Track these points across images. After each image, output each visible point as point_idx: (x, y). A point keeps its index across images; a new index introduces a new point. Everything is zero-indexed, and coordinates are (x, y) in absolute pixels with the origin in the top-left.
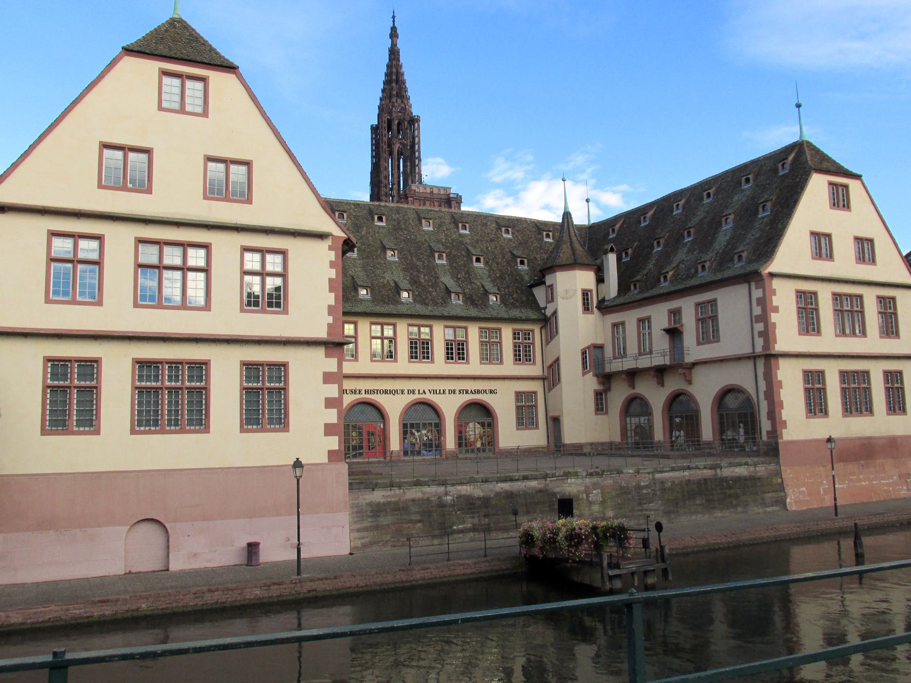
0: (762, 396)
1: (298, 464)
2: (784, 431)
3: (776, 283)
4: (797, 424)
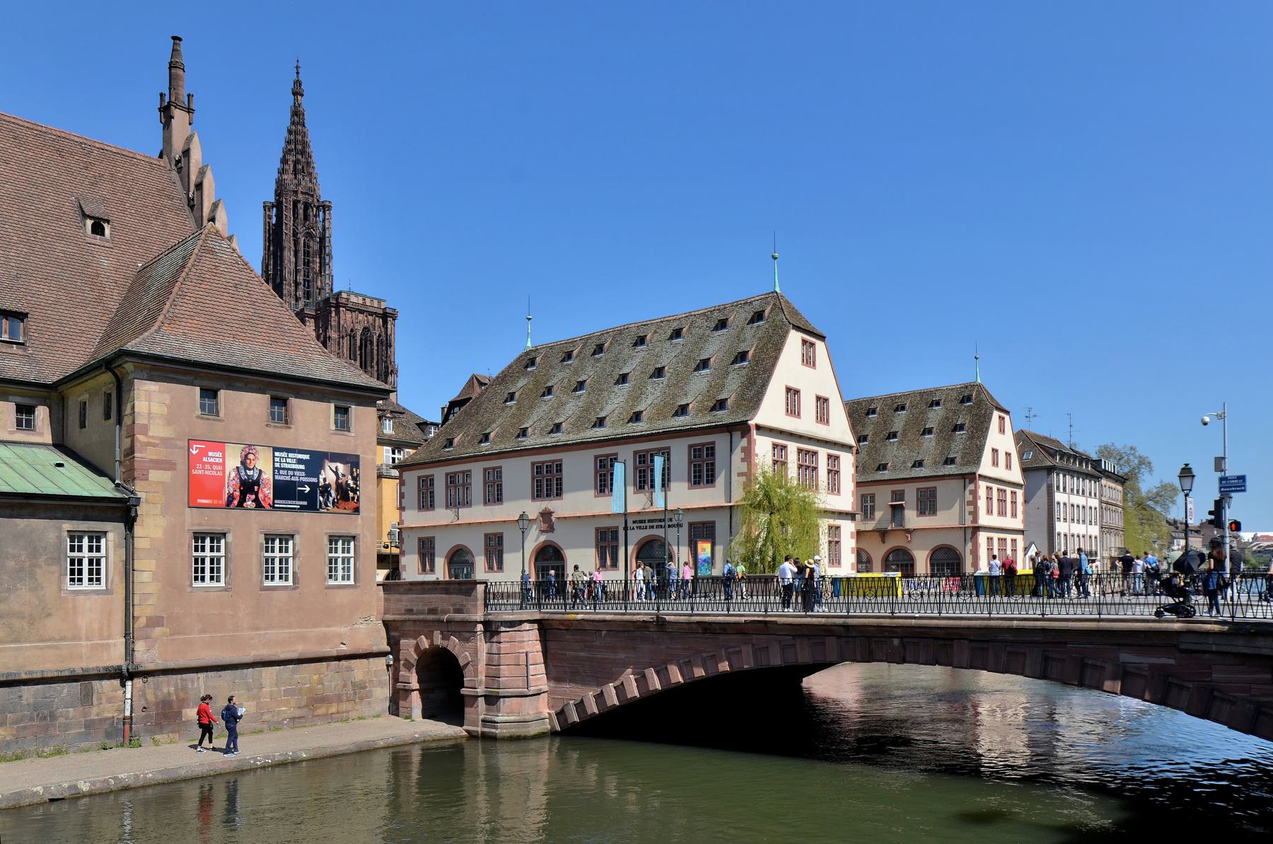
0: (968, 552)
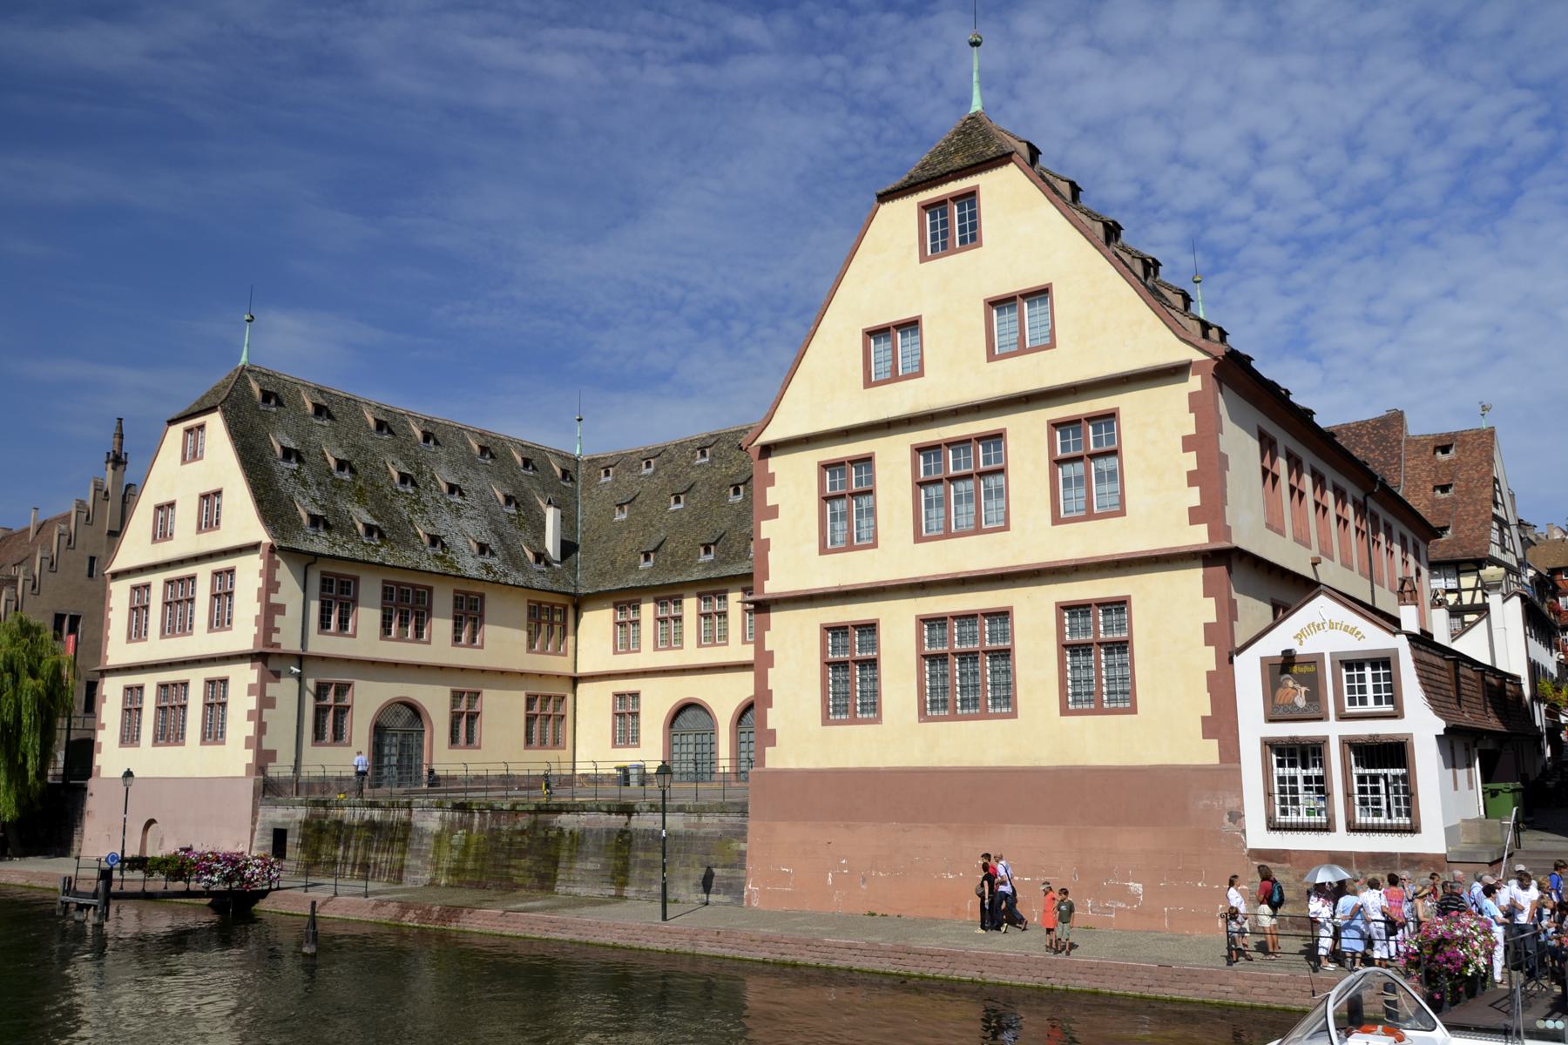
1: (129, 774)
2: (768, 750)
3: (775, 463)
4: (803, 738)
